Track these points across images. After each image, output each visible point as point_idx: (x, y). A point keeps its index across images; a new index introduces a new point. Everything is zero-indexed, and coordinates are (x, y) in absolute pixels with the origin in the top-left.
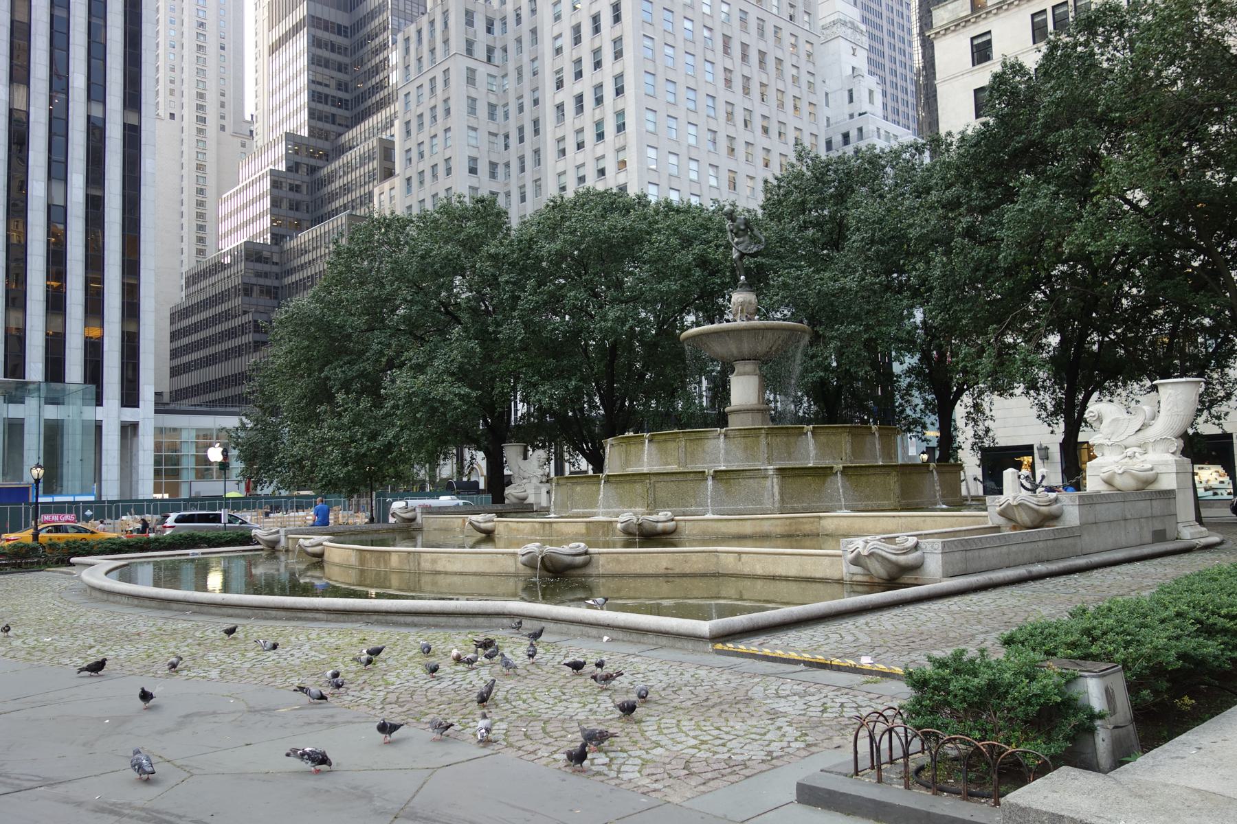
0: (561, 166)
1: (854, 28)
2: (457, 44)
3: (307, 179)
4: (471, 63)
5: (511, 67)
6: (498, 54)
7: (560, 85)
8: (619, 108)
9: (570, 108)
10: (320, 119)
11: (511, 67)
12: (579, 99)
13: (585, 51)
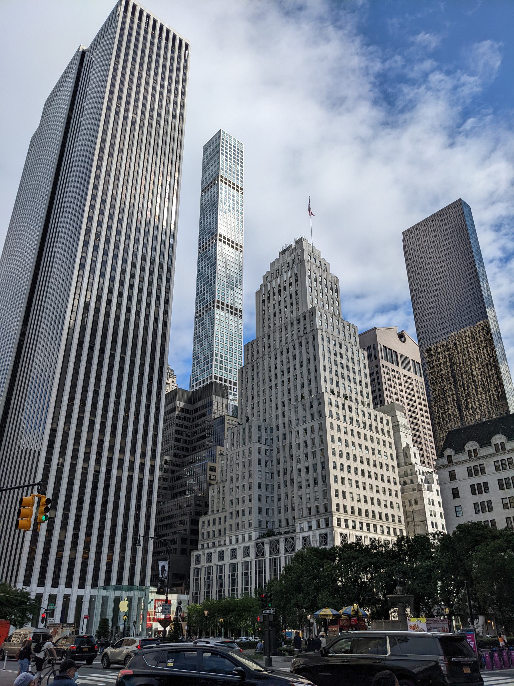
0: (300, 493)
1: (406, 427)
2: (255, 438)
3: (171, 475)
4: (259, 445)
5: (274, 447)
6: (269, 441)
7: (299, 461)
8: (324, 474)
9: (303, 471)
10: (178, 449)
11: (274, 447)
12: (307, 468)
13: (309, 450)
